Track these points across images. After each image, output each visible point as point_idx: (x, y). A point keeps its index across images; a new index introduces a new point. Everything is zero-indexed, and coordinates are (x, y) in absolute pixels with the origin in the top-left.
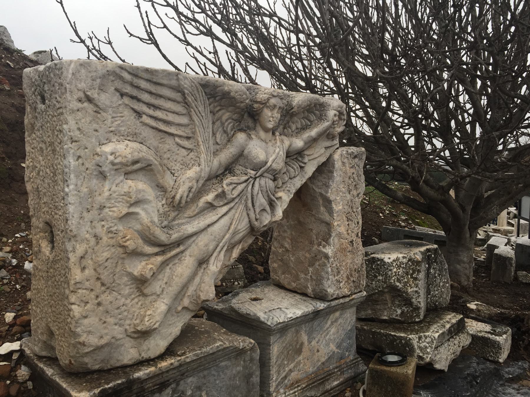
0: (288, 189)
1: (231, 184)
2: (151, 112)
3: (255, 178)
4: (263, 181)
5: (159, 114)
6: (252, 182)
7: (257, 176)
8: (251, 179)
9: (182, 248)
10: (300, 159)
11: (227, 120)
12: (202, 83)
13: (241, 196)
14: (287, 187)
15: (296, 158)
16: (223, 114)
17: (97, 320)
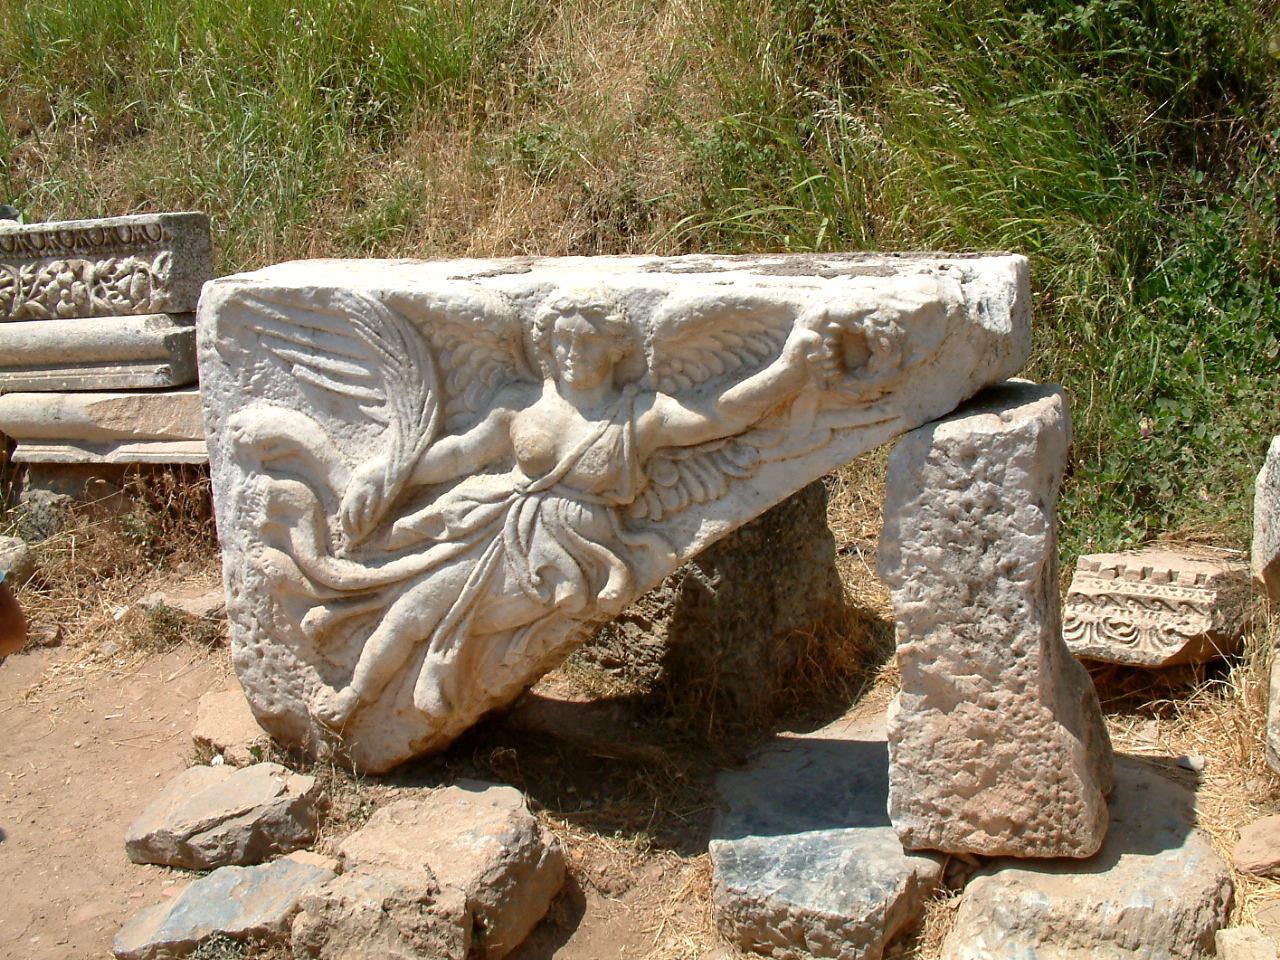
0: (687, 527)
1: (465, 499)
2: (307, 358)
3: (529, 494)
4: (550, 503)
5: (321, 361)
6: (518, 502)
7: (530, 489)
8: (516, 495)
9: (375, 605)
10: (729, 455)
11: (482, 363)
12: (386, 299)
13: (492, 526)
14: (684, 522)
15: (719, 451)
16: (471, 352)
17: (260, 672)
